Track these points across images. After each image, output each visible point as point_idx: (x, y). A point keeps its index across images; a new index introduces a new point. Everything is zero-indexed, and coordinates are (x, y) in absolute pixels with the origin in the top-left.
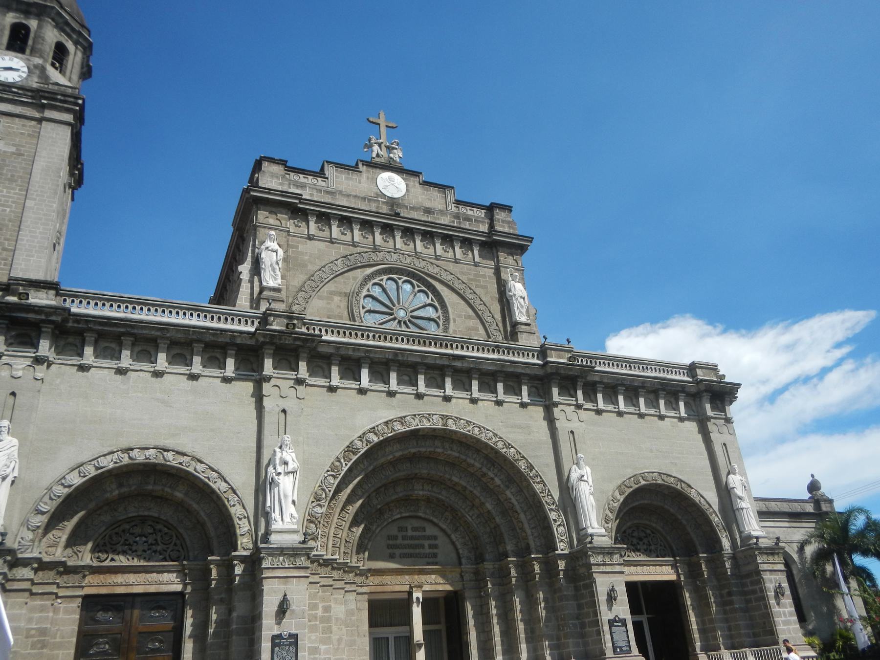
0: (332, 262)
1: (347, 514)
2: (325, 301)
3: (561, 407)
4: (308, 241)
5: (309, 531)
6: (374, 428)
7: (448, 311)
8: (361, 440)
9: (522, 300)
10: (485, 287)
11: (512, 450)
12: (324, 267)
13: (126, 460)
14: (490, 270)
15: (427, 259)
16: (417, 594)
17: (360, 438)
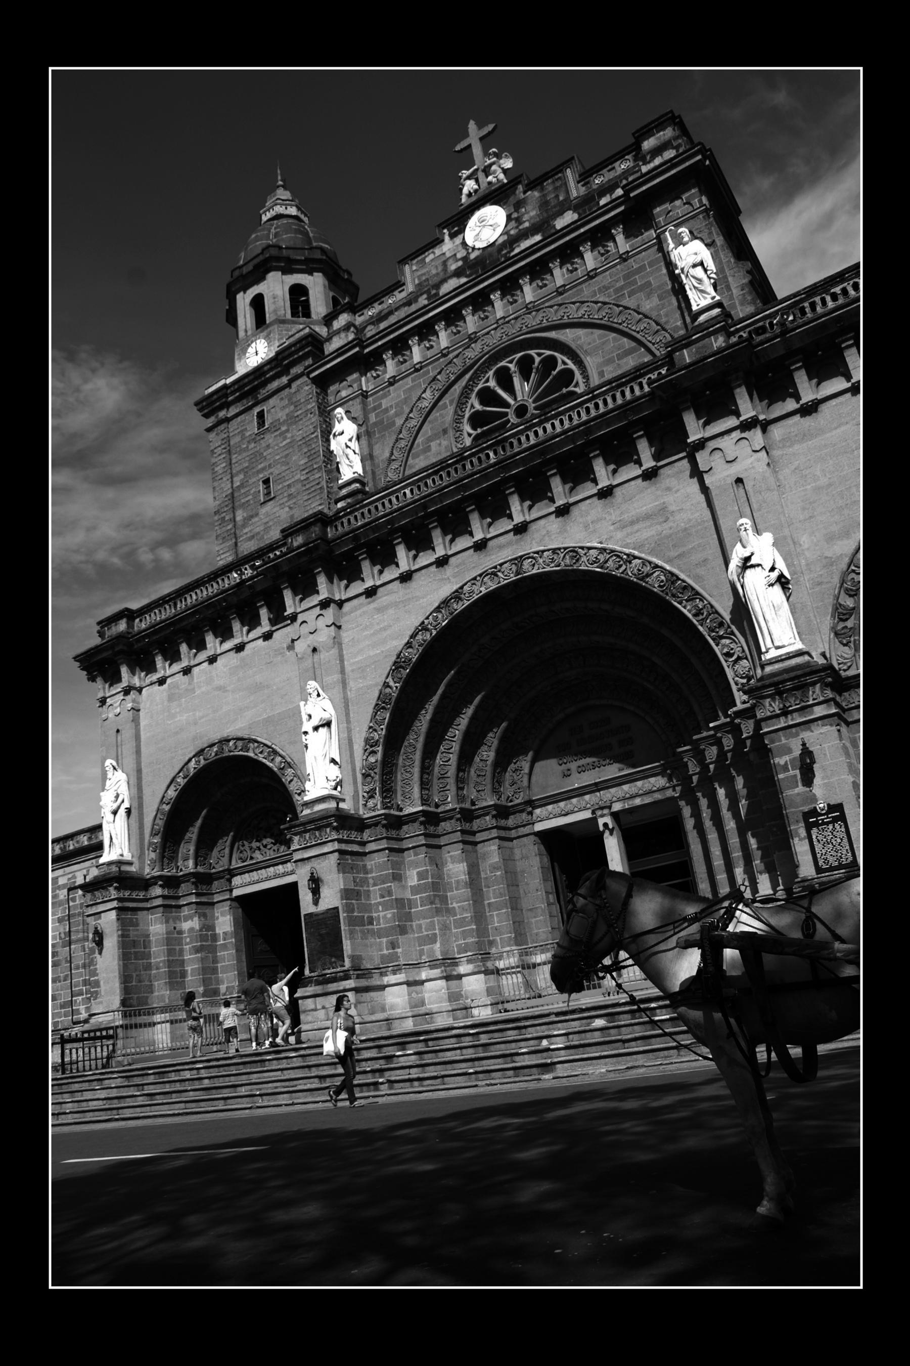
0: (419, 399)
1: (454, 744)
2: (422, 457)
3: (712, 445)
4: (391, 388)
5: (367, 789)
6: (423, 623)
7: (585, 367)
8: (411, 647)
9: (699, 268)
10: (649, 284)
11: (636, 562)
12: (411, 411)
13: (203, 762)
14: (649, 251)
15: (547, 305)
16: (605, 820)
17: (409, 645)
